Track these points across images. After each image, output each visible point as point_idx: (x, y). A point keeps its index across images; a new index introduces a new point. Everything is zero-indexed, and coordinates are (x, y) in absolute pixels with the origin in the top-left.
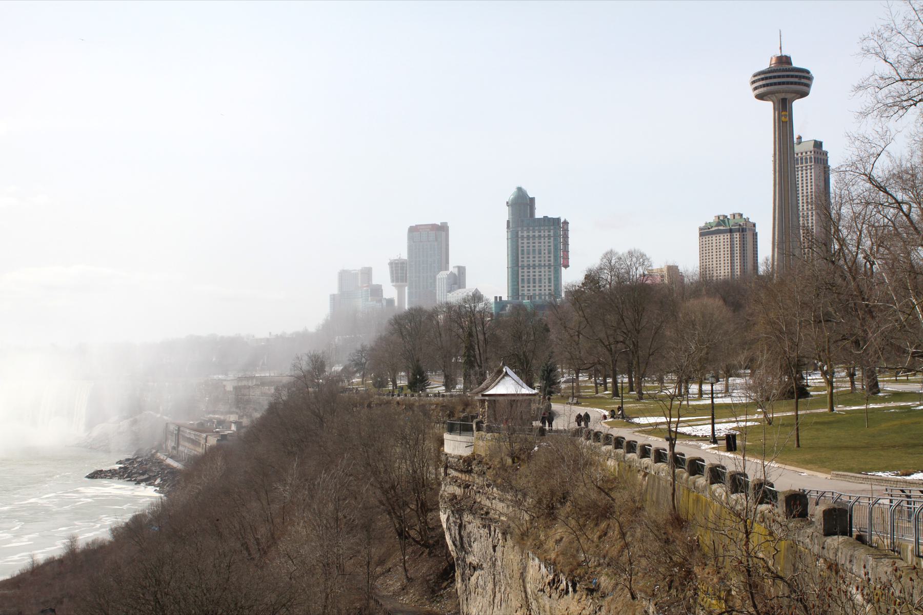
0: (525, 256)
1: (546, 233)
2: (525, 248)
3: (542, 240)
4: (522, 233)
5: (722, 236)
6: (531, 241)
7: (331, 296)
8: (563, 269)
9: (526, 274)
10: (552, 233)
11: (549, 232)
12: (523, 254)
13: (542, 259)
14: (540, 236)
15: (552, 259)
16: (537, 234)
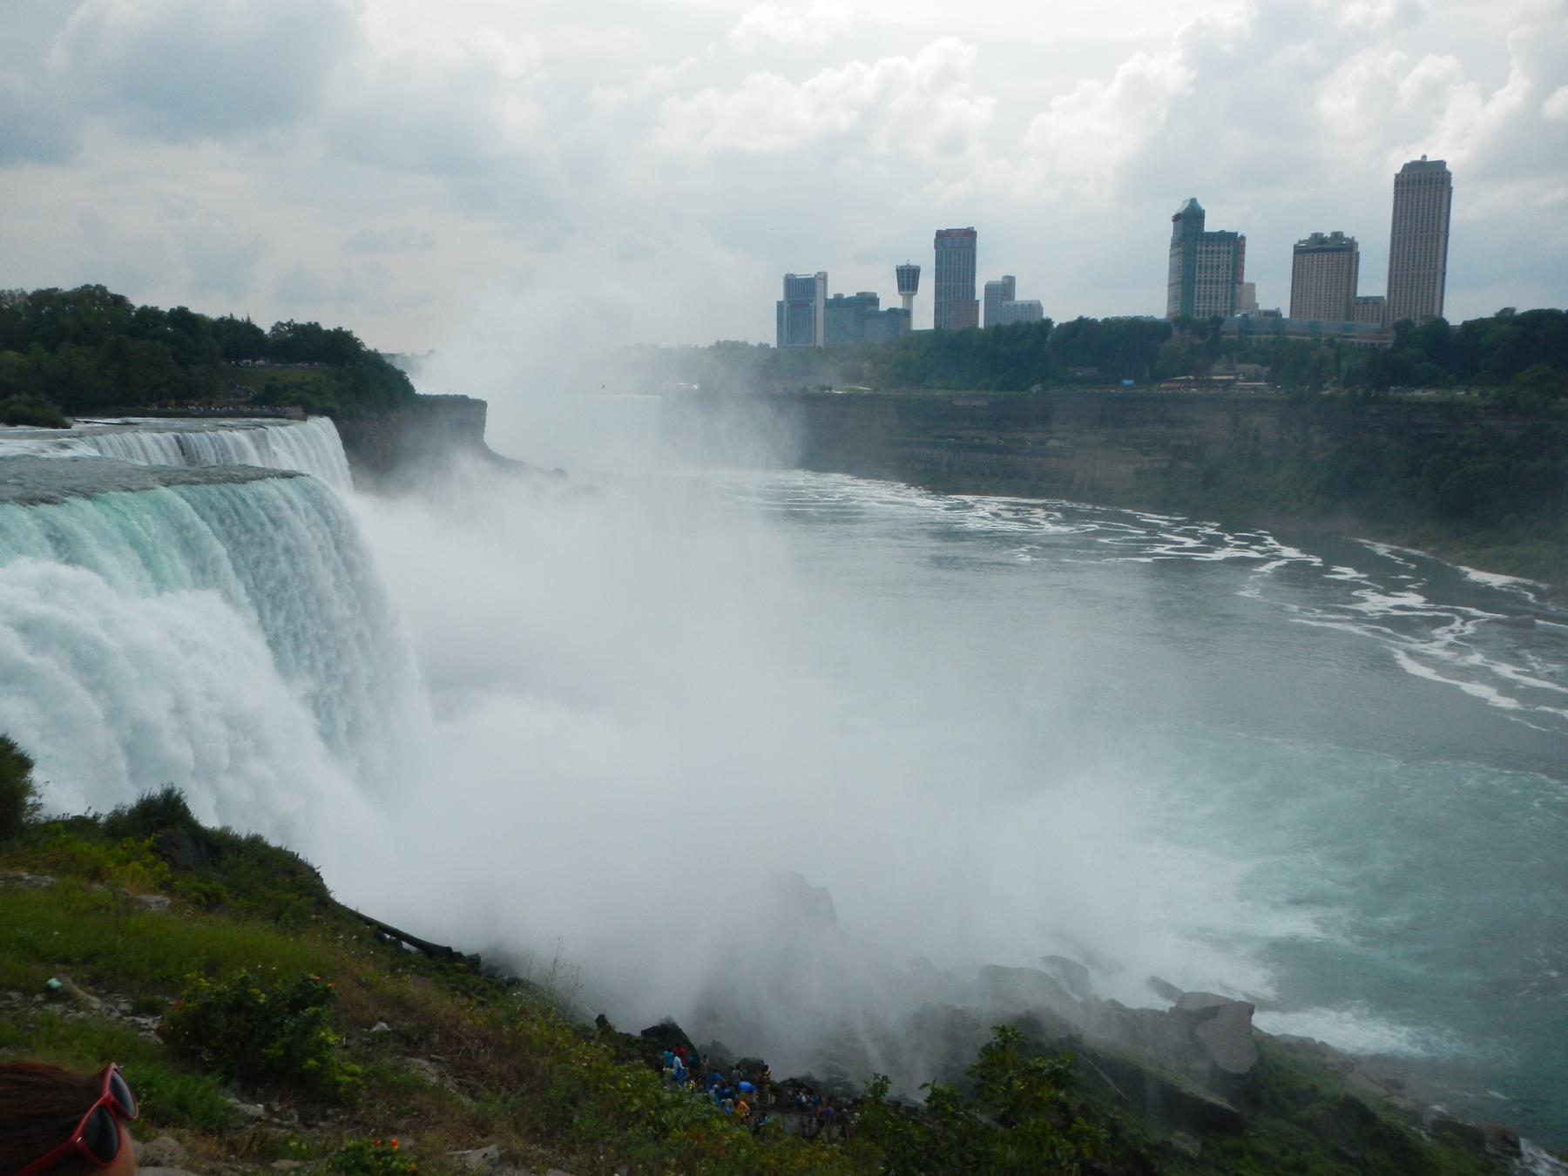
0: (1203, 271)
1: (1226, 248)
2: (1203, 264)
3: (1221, 256)
4: (1201, 246)
5: (1326, 255)
6: (1210, 255)
7: (778, 302)
8: (1237, 285)
9: (1202, 289)
10: (1231, 249)
11: (1229, 246)
12: (1200, 268)
13: (1220, 274)
14: (1219, 252)
15: (1230, 275)
16: (1216, 248)
